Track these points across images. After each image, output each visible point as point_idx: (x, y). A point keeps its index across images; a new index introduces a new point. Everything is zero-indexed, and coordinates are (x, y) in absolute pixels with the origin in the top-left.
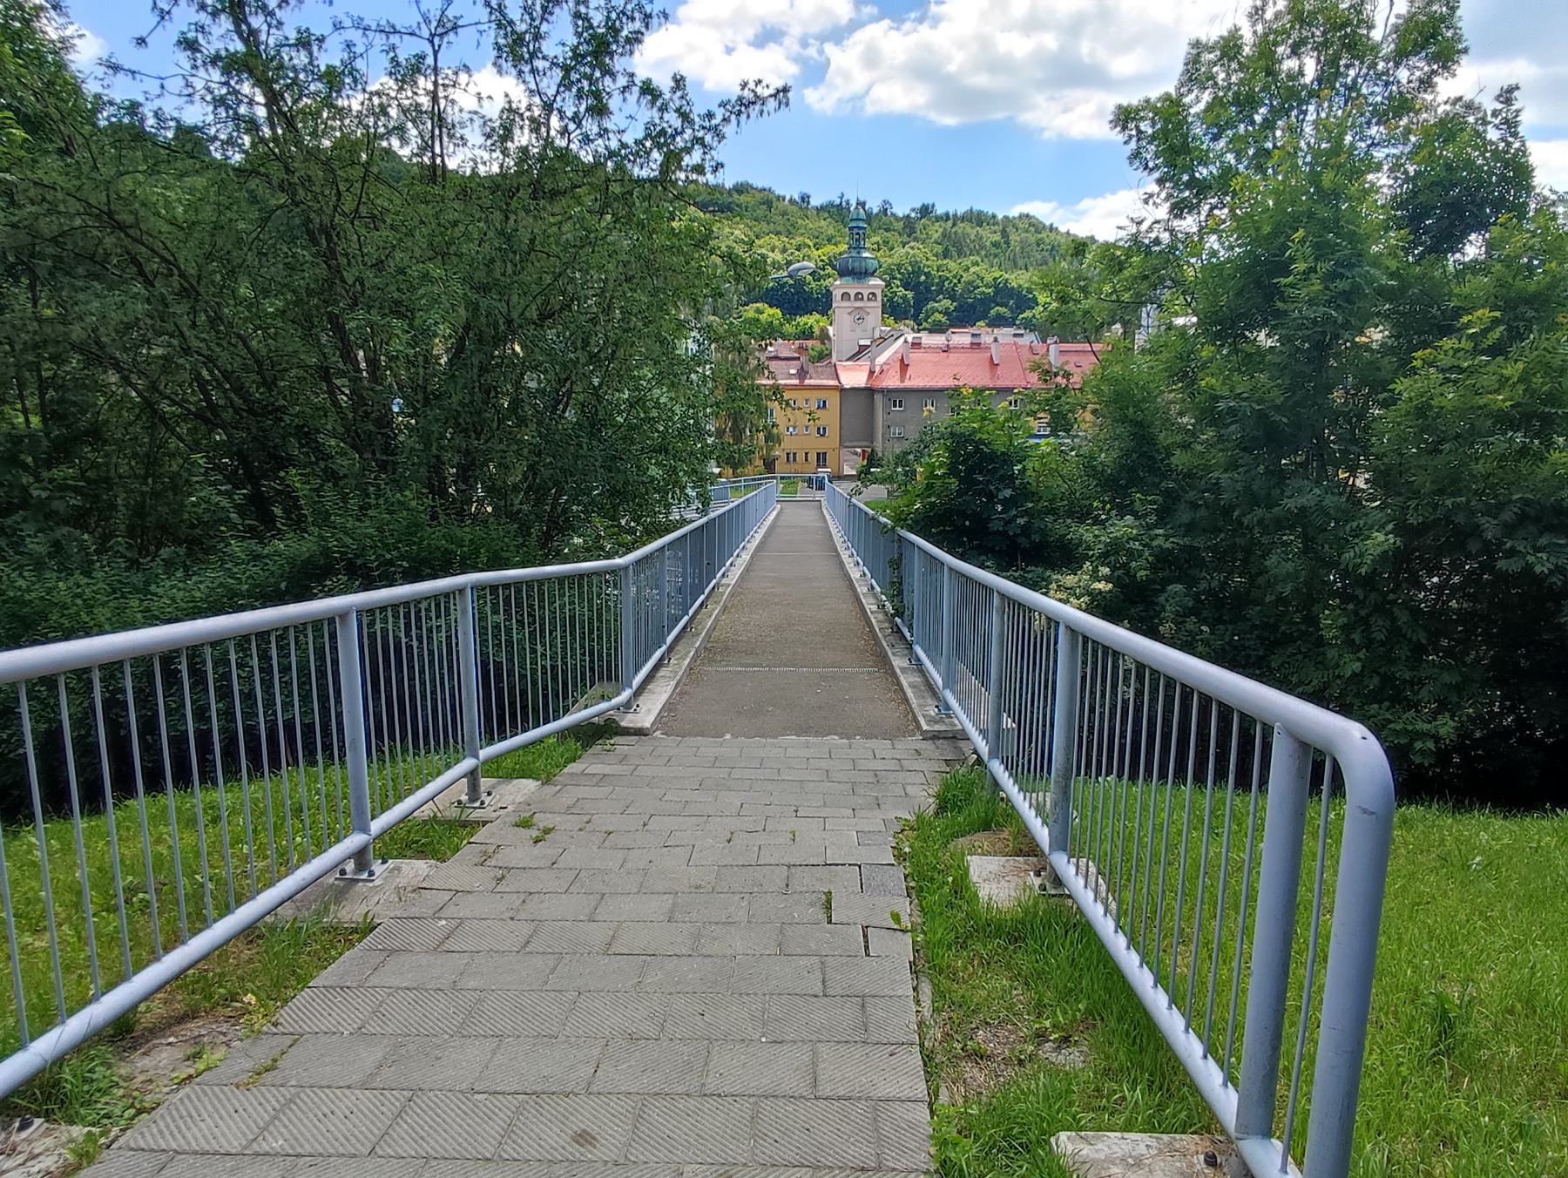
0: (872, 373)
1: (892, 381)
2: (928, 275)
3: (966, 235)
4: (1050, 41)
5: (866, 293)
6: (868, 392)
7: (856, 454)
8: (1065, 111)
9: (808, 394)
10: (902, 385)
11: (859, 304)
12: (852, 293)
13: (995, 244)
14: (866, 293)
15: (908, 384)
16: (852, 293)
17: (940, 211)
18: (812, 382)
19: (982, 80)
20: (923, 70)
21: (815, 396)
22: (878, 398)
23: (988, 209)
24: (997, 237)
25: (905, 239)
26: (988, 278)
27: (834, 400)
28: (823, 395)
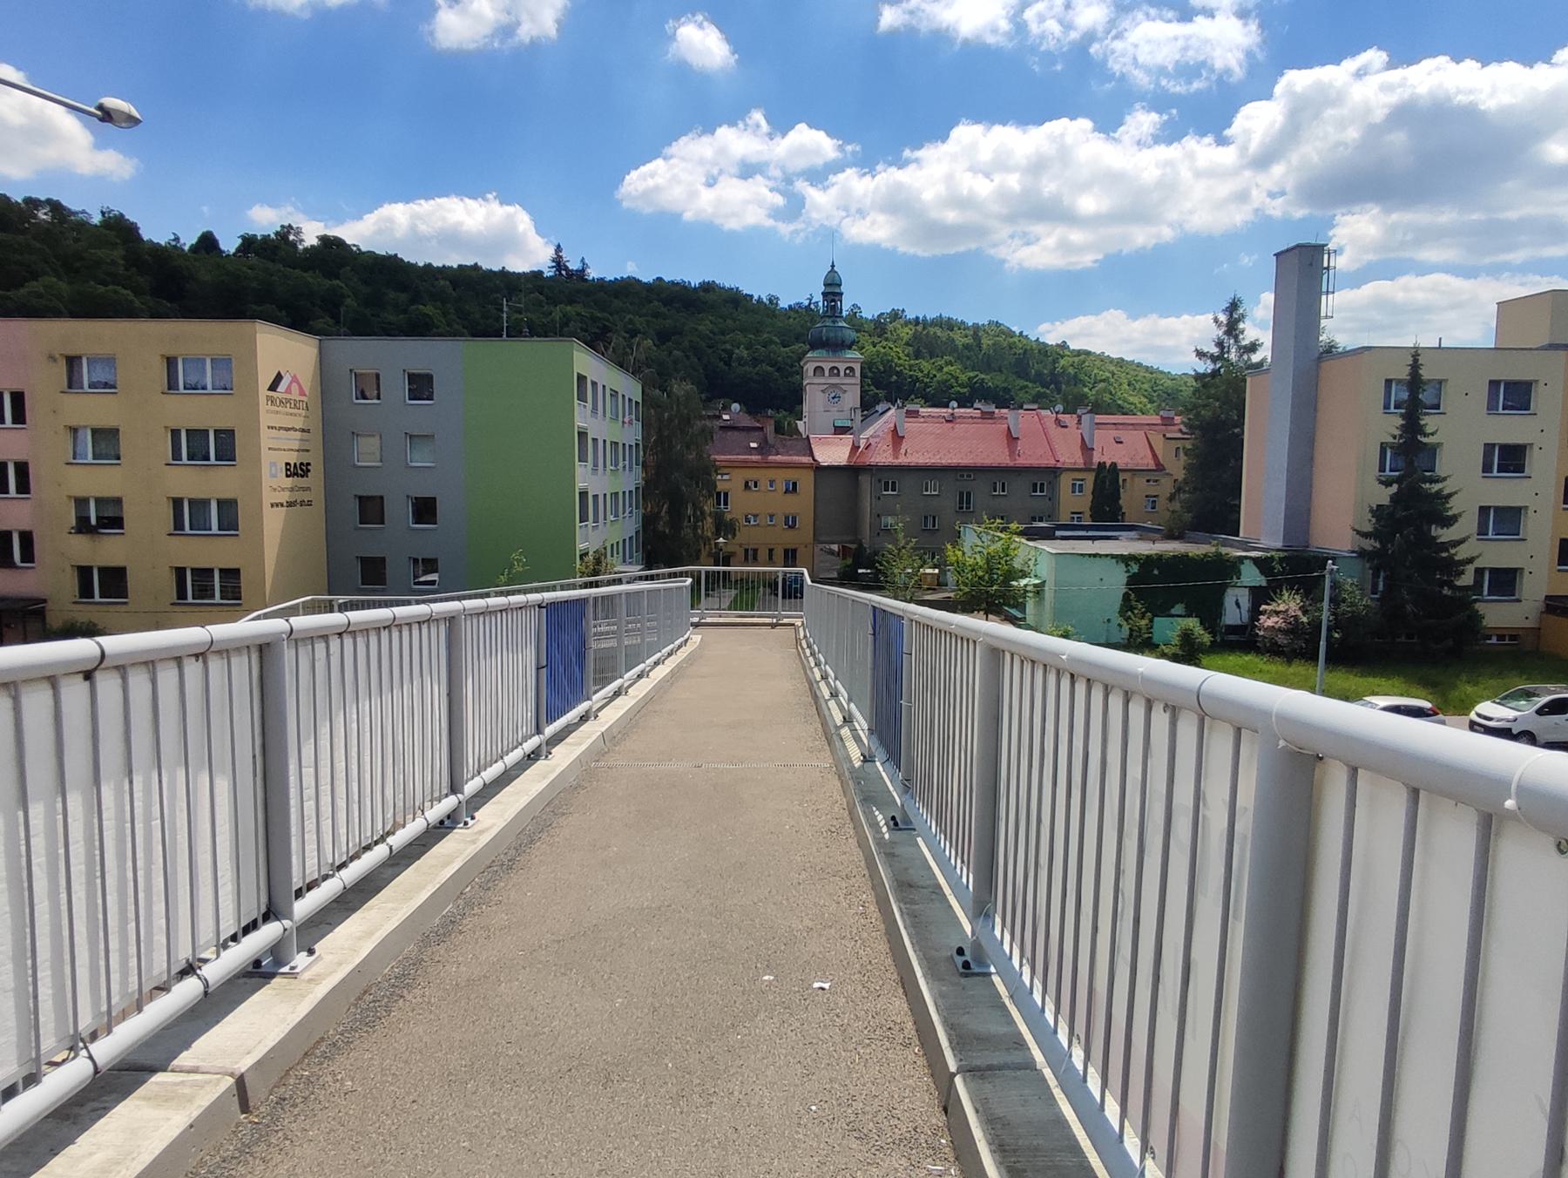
0: (855, 448)
1: (882, 456)
2: (899, 374)
3: (936, 337)
4: (1013, 182)
5: (842, 366)
6: (852, 472)
7: (832, 552)
8: (1028, 244)
9: (771, 474)
10: (897, 462)
11: (835, 380)
12: (827, 366)
13: (966, 347)
14: (842, 366)
15: (902, 460)
16: (827, 366)
17: (910, 315)
18: (779, 458)
19: (951, 216)
20: (897, 204)
21: (782, 477)
22: (865, 480)
23: (958, 316)
24: (969, 341)
25: (876, 340)
26: (963, 378)
27: (806, 481)
28: (792, 475)
